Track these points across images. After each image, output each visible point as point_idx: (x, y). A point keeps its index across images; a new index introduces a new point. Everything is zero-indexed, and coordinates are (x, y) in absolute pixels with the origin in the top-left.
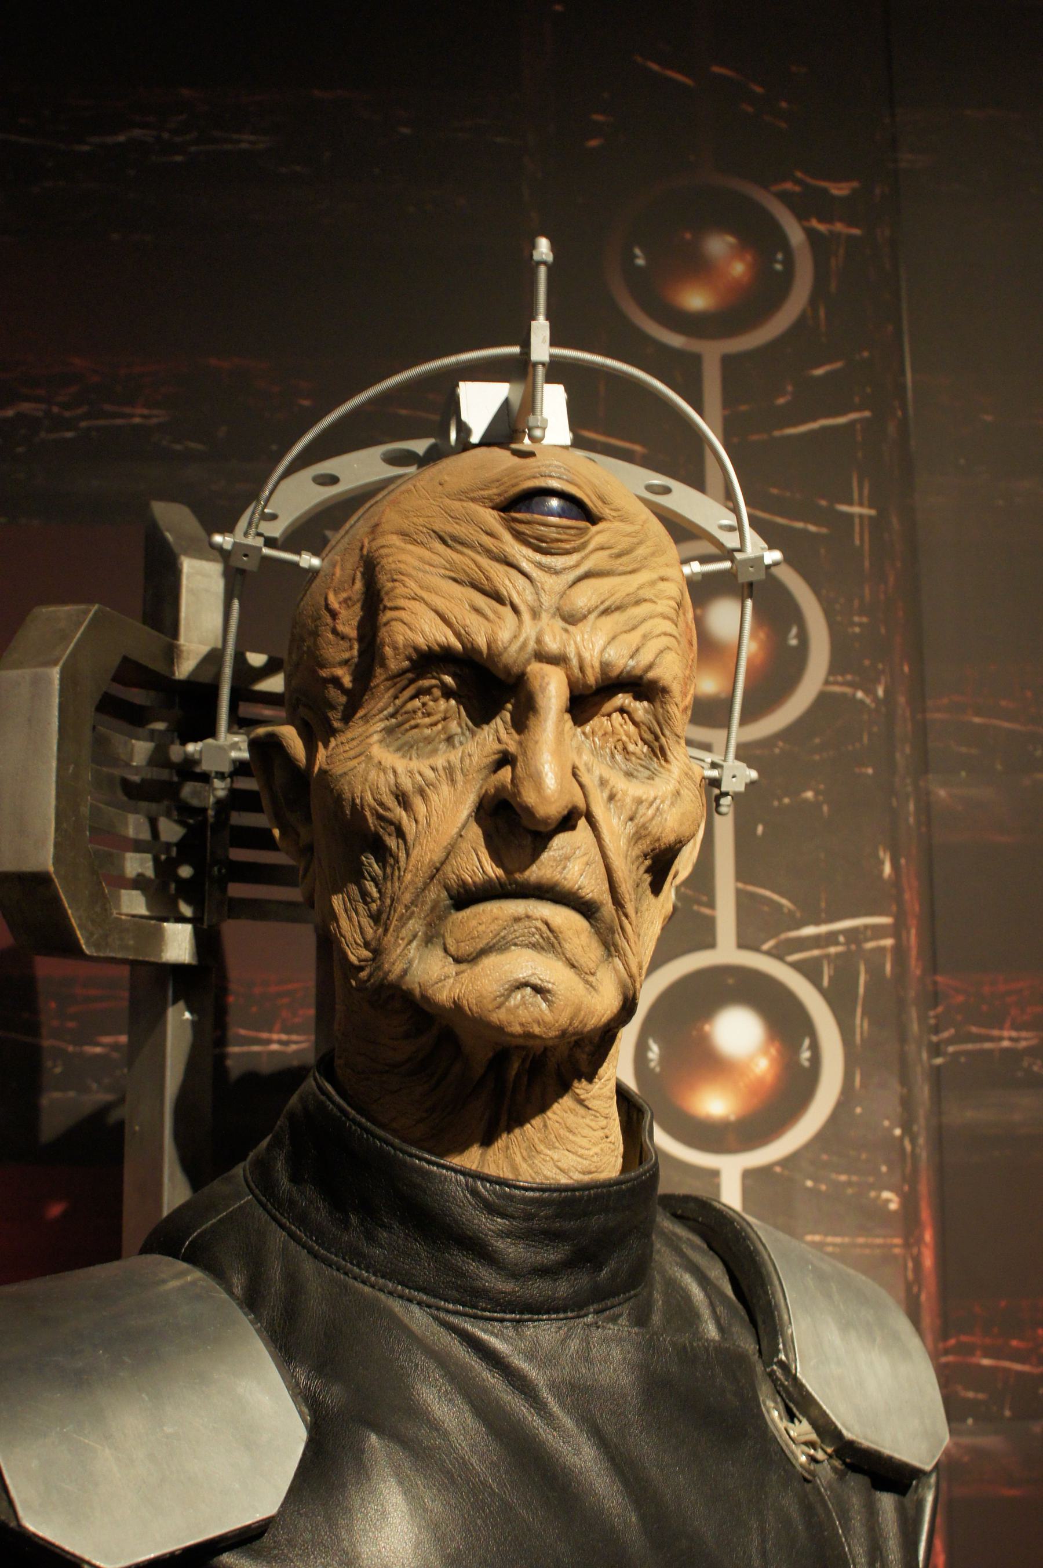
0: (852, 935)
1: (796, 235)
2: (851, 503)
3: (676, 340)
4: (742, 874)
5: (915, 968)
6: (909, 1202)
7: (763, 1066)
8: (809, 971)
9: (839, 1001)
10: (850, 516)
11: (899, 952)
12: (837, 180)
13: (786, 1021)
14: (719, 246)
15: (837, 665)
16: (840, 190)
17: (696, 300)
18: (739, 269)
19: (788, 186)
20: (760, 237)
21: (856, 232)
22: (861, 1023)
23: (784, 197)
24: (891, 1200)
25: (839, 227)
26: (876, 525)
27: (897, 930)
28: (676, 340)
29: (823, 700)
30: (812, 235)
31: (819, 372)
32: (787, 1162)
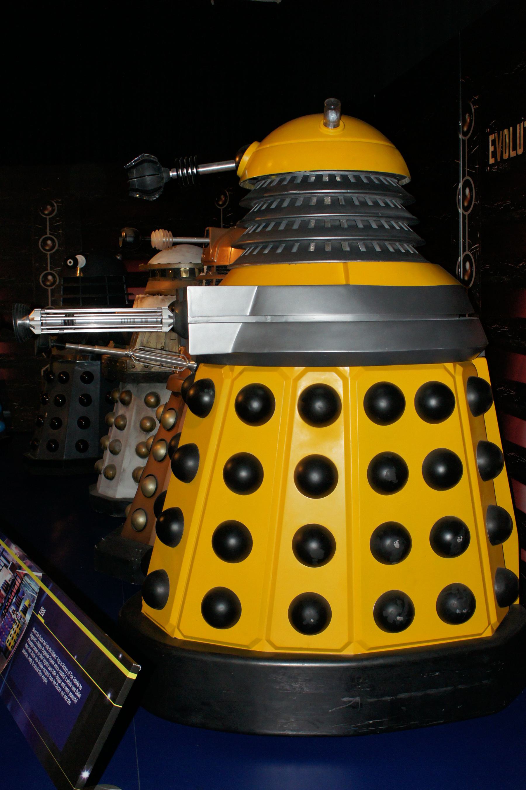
1: (55, 205)
3: (44, 216)
4: (51, 264)
7: (52, 280)
13: (54, 277)
14: (49, 207)
15: (59, 246)
17: (46, 212)
18: (50, 209)
20: (52, 206)
28: (44, 216)
30: (57, 205)
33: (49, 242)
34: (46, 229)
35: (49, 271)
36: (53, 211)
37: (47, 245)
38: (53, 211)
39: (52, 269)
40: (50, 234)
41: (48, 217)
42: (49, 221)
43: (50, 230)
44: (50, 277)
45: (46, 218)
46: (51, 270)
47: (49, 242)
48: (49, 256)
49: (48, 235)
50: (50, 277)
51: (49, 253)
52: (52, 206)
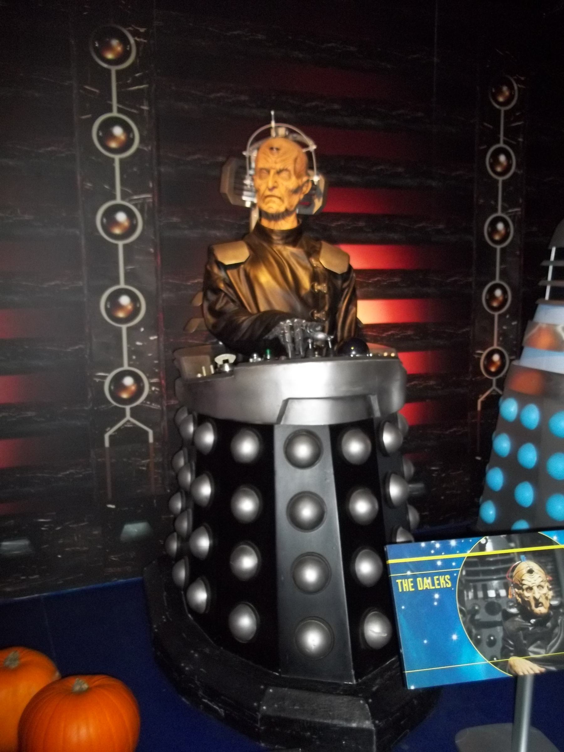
0: (144, 199)
1: (132, 40)
2: (143, 105)
3: (105, 65)
5: (156, 205)
6: (155, 250)
8: (136, 205)
9: (142, 211)
10: (143, 110)
11: (153, 202)
12: (142, 27)
13: (131, 215)
14: (115, 42)
16: (142, 30)
17: (110, 56)
19: (130, 28)
20: (124, 41)
21: (145, 41)
22: (146, 216)
23: (129, 31)
24: (152, 250)
25: (142, 40)
26: (149, 112)
27: (153, 198)
28: (105, 65)
29: (138, 150)
30: (136, 41)
31: (137, 75)
32: (132, 243)
33: (118, 131)
34: (110, 99)
35: (119, 200)
36: (125, 56)
37: (113, 137)
38: (125, 56)
39: (124, 196)
40: (120, 111)
41: (114, 69)
42: (118, 79)
43: (119, 102)
44: (121, 217)
45: (109, 71)
46: (123, 198)
47: (118, 131)
48: (117, 165)
49: (115, 114)
50: (121, 217)
51: (117, 158)
52: (124, 41)
